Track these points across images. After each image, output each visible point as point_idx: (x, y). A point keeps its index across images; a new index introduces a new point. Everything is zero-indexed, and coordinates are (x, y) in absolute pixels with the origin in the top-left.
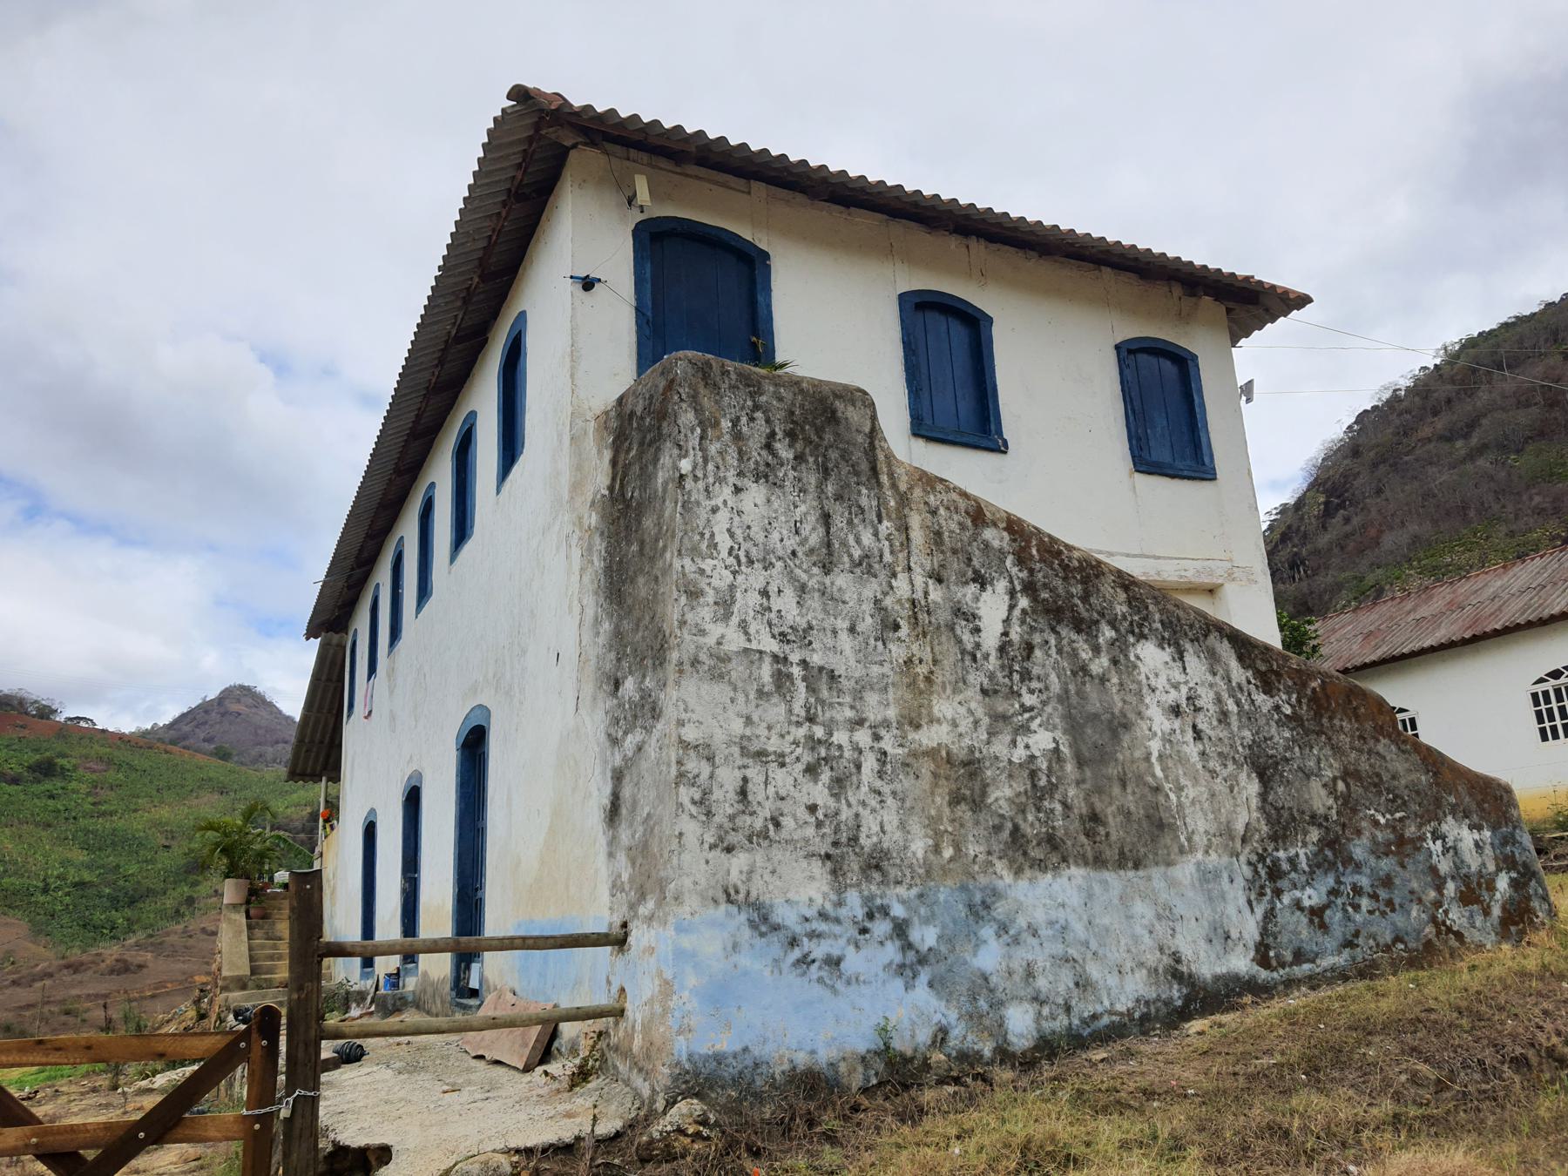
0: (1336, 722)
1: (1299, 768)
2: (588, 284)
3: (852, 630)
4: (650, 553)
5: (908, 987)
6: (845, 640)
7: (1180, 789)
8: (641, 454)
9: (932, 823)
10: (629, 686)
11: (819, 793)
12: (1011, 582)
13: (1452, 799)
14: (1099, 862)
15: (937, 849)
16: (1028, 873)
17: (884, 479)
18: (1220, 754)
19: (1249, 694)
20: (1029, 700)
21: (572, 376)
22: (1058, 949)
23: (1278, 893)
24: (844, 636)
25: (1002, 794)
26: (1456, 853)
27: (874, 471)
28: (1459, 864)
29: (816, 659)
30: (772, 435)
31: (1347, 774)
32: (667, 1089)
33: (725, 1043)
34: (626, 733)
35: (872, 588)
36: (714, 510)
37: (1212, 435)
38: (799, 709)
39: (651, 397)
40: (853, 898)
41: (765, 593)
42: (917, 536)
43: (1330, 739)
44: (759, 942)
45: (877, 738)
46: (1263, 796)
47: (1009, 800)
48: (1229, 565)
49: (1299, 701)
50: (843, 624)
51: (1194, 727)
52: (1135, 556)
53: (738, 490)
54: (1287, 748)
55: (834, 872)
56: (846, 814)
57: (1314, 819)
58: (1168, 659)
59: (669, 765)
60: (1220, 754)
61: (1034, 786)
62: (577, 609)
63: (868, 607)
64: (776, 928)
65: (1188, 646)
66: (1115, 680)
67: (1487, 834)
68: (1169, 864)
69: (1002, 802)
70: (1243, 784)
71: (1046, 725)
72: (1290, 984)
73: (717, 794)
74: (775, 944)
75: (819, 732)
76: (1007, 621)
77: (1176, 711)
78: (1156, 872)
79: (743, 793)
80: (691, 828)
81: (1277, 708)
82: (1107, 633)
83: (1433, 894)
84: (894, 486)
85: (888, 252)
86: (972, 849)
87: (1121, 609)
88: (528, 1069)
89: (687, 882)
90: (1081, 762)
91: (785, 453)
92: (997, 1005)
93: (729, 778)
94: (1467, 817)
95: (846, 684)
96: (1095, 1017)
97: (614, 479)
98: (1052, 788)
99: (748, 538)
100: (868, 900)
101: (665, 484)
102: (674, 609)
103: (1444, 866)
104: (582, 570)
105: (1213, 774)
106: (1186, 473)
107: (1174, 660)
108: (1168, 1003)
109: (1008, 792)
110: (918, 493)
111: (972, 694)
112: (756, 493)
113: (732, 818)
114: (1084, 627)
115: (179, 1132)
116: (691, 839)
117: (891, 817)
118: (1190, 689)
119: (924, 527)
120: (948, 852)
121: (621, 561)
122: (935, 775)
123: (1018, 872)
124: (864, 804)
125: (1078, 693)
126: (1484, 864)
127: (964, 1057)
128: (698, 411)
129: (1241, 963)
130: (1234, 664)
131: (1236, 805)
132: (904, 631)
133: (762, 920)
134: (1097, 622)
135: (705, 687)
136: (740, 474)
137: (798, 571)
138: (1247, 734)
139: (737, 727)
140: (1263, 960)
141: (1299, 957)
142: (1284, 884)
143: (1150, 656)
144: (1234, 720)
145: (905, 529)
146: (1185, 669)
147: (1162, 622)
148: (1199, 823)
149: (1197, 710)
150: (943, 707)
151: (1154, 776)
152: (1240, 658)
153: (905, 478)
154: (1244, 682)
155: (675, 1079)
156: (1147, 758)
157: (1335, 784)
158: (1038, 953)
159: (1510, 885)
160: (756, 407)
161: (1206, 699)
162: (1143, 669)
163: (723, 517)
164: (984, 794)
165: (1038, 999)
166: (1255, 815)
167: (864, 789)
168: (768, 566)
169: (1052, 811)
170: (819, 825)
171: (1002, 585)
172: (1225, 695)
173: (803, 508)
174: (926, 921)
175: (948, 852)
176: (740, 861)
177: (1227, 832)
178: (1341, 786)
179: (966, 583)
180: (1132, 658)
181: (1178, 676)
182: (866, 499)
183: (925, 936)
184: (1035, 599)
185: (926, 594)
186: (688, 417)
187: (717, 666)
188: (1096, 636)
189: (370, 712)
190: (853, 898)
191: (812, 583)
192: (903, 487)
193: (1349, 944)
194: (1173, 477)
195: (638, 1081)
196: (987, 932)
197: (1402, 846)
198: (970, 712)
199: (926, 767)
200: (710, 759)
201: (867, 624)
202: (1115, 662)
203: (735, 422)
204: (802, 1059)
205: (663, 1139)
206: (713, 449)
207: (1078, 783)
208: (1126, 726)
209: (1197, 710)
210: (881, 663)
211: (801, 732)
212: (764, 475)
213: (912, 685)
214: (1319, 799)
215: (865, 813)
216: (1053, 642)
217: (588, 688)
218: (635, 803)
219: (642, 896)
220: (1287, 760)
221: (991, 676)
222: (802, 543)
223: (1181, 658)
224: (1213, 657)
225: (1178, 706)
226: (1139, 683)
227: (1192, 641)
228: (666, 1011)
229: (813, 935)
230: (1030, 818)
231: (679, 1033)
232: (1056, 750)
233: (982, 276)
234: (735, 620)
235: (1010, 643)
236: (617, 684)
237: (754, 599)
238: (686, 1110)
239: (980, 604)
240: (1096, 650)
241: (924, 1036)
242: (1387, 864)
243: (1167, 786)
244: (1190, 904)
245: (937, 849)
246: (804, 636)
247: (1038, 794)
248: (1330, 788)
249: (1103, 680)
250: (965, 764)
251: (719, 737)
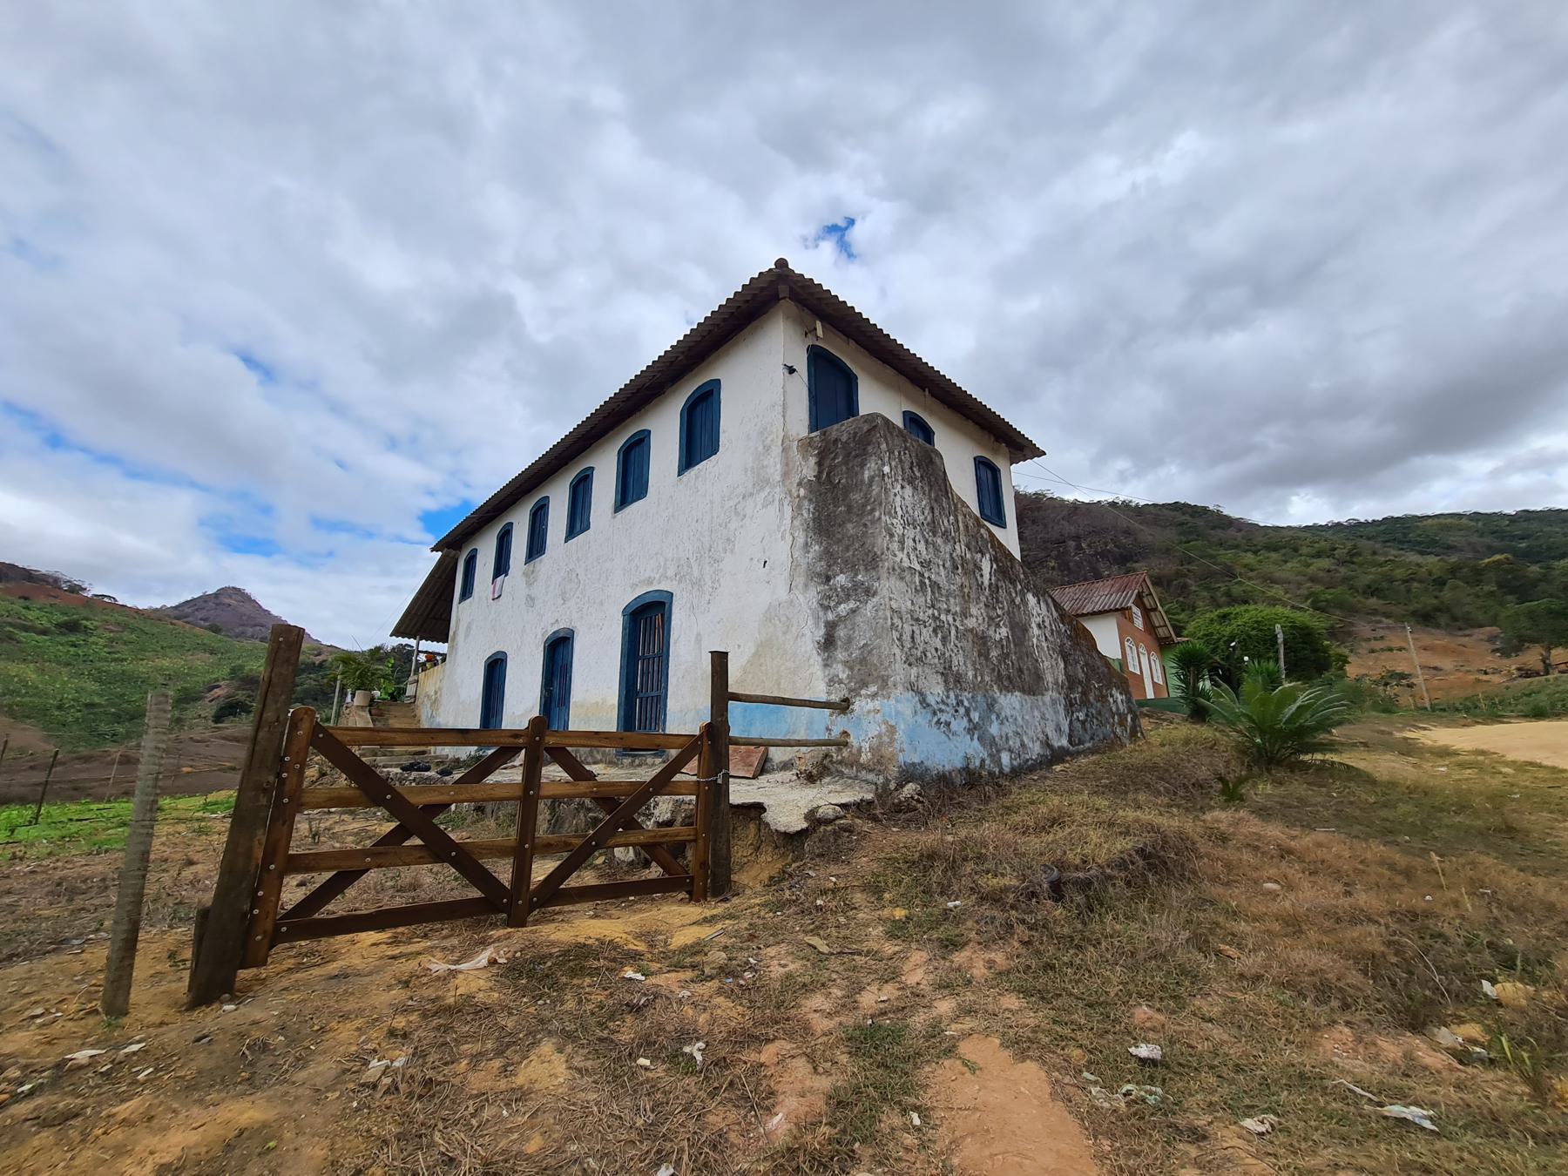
2: (791, 370)
3: (944, 565)
4: (861, 512)
5: (972, 739)
6: (943, 573)
8: (845, 462)
9: (974, 664)
10: (841, 579)
11: (938, 643)
14: (1023, 691)
15: (976, 677)
16: (1004, 692)
20: (999, 612)
21: (784, 416)
22: (1014, 729)
23: (1073, 713)
24: (941, 567)
25: (994, 654)
28: (1118, 709)
30: (912, 463)
31: (1087, 664)
32: (896, 778)
33: (917, 760)
34: (839, 603)
35: (948, 548)
36: (895, 495)
38: (929, 601)
39: (856, 433)
40: (952, 694)
41: (914, 540)
44: (924, 711)
45: (955, 620)
50: (941, 563)
53: (903, 487)
55: (945, 681)
56: (947, 655)
57: (1080, 682)
59: (886, 619)
62: (789, 539)
63: (948, 556)
64: (928, 705)
68: (1043, 695)
72: (1079, 753)
73: (904, 637)
74: (929, 710)
75: (936, 614)
78: (1040, 697)
79: (913, 638)
80: (897, 651)
85: (898, 390)
86: (987, 678)
87: (1022, 576)
88: (754, 778)
89: (898, 678)
90: (1015, 645)
91: (918, 474)
92: (999, 751)
93: (907, 629)
95: (944, 592)
96: (1028, 760)
97: (820, 472)
98: (1008, 655)
100: (957, 696)
101: (872, 479)
102: (882, 541)
103: (1114, 709)
104: (793, 519)
108: (1046, 756)
109: (995, 654)
111: (982, 605)
112: (909, 491)
113: (910, 649)
114: (1013, 582)
115: (668, 789)
116: (898, 657)
117: (961, 659)
120: (979, 679)
121: (829, 515)
123: (1001, 692)
124: (952, 650)
127: (991, 774)
128: (887, 444)
129: (1064, 742)
132: (960, 571)
133: (924, 703)
135: (898, 583)
136: (903, 479)
139: (909, 603)
140: (1070, 742)
141: (1081, 742)
142: (1074, 709)
143: (1030, 597)
145: (957, 521)
148: (1049, 678)
150: (974, 611)
155: (900, 773)
158: (1009, 729)
160: (906, 448)
161: (1047, 624)
163: (898, 499)
164: (989, 654)
165: (1010, 751)
168: (915, 528)
170: (939, 659)
171: (988, 556)
173: (924, 502)
174: (975, 710)
175: (979, 679)
176: (914, 671)
177: (1056, 683)
183: (975, 716)
184: (997, 565)
186: (884, 446)
187: (900, 572)
189: (499, 596)
190: (952, 694)
191: (930, 539)
193: (1092, 738)
195: (871, 777)
196: (994, 717)
197: (1102, 698)
200: (901, 619)
201: (948, 564)
203: (899, 453)
204: (940, 768)
205: (906, 801)
206: (893, 463)
208: (1027, 630)
213: (963, 597)
214: (1081, 675)
217: (800, 580)
218: (850, 640)
219: (865, 685)
222: (926, 519)
228: (892, 741)
229: (941, 711)
231: (900, 751)
233: (931, 412)
234: (905, 552)
236: (828, 579)
237: (911, 543)
238: (910, 789)
241: (978, 763)
242: (1099, 705)
244: (1049, 714)
245: (975, 676)
246: (926, 564)
250: (982, 638)
251: (904, 609)
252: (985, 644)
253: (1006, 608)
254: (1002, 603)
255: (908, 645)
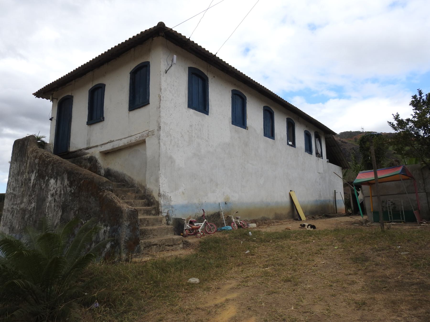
0: (83, 193)
1: (70, 208)
7: (49, 215)
12: (36, 171)
13: (102, 216)
17: (26, 154)
18: (57, 206)
19: (67, 188)
26: (98, 234)
27: (26, 154)
29: (15, 193)
31: (80, 209)
36: (12, 169)
37: (150, 89)
42: (28, 165)
43: (79, 198)
45: (17, 207)
46: (62, 215)
47: (27, 218)
48: (147, 131)
49: (76, 188)
51: (55, 198)
52: (127, 138)
54: (70, 202)
58: (55, 182)
60: (57, 206)
61: (30, 215)
63: (21, 182)
65: (59, 178)
66: (45, 190)
67: (109, 228)
69: (26, 218)
70: (59, 213)
71: (34, 202)
73: (4, 218)
76: (34, 180)
77: (52, 195)
79: (6, 217)
81: (71, 191)
82: (47, 178)
83: (89, 246)
84: (27, 155)
87: (50, 171)
93: (6, 214)
94: (104, 222)
95: (17, 197)
99: (13, 172)
105: (55, 210)
106: (141, 105)
107: (55, 182)
110: (30, 155)
111: (28, 196)
112: (15, 163)
114: (43, 178)
117: (16, 221)
118: (56, 189)
119: (29, 162)
122: (21, 213)
125: (40, 194)
126: (104, 239)
130: (66, 180)
131: (56, 218)
134: (45, 176)
137: (16, 177)
138: (63, 199)
139: (8, 206)
143: (52, 181)
144: (62, 197)
146: (57, 184)
147: (56, 173)
149: (56, 194)
150: (25, 200)
151: (46, 211)
152: (69, 179)
153: (29, 153)
154: (67, 184)
156: (46, 208)
157: (76, 212)
159: (110, 247)
162: (50, 186)
163: (12, 169)
166: (59, 221)
167: (14, 216)
169: (31, 220)
171: (35, 172)
172: (62, 189)
176: (4, 228)
178: (77, 212)
179: (31, 173)
180: (49, 183)
181: (55, 186)
182: (24, 160)
185: (27, 177)
188: (45, 179)
191: (17, 179)
192: (28, 155)
194: (140, 107)
198: (27, 200)
199: (21, 211)
200: (5, 211)
202: (46, 185)
206: (13, 157)
207: (36, 214)
209: (56, 194)
210: (20, 192)
211: (11, 206)
212: (16, 160)
215: (14, 220)
216: (39, 182)
220: (69, 206)
221: (30, 192)
223: (57, 182)
224: (63, 180)
225: (53, 194)
226: (48, 189)
227: (60, 176)
230: (28, 222)
232: (34, 206)
235: (34, 184)
239: (32, 177)
240: (44, 183)
243: (47, 214)
245: (18, 227)
247: (31, 216)
248: (75, 213)
249: (44, 189)
252: (25, 213)
253: (37, 193)
254: (35, 191)
255: (5, 220)
